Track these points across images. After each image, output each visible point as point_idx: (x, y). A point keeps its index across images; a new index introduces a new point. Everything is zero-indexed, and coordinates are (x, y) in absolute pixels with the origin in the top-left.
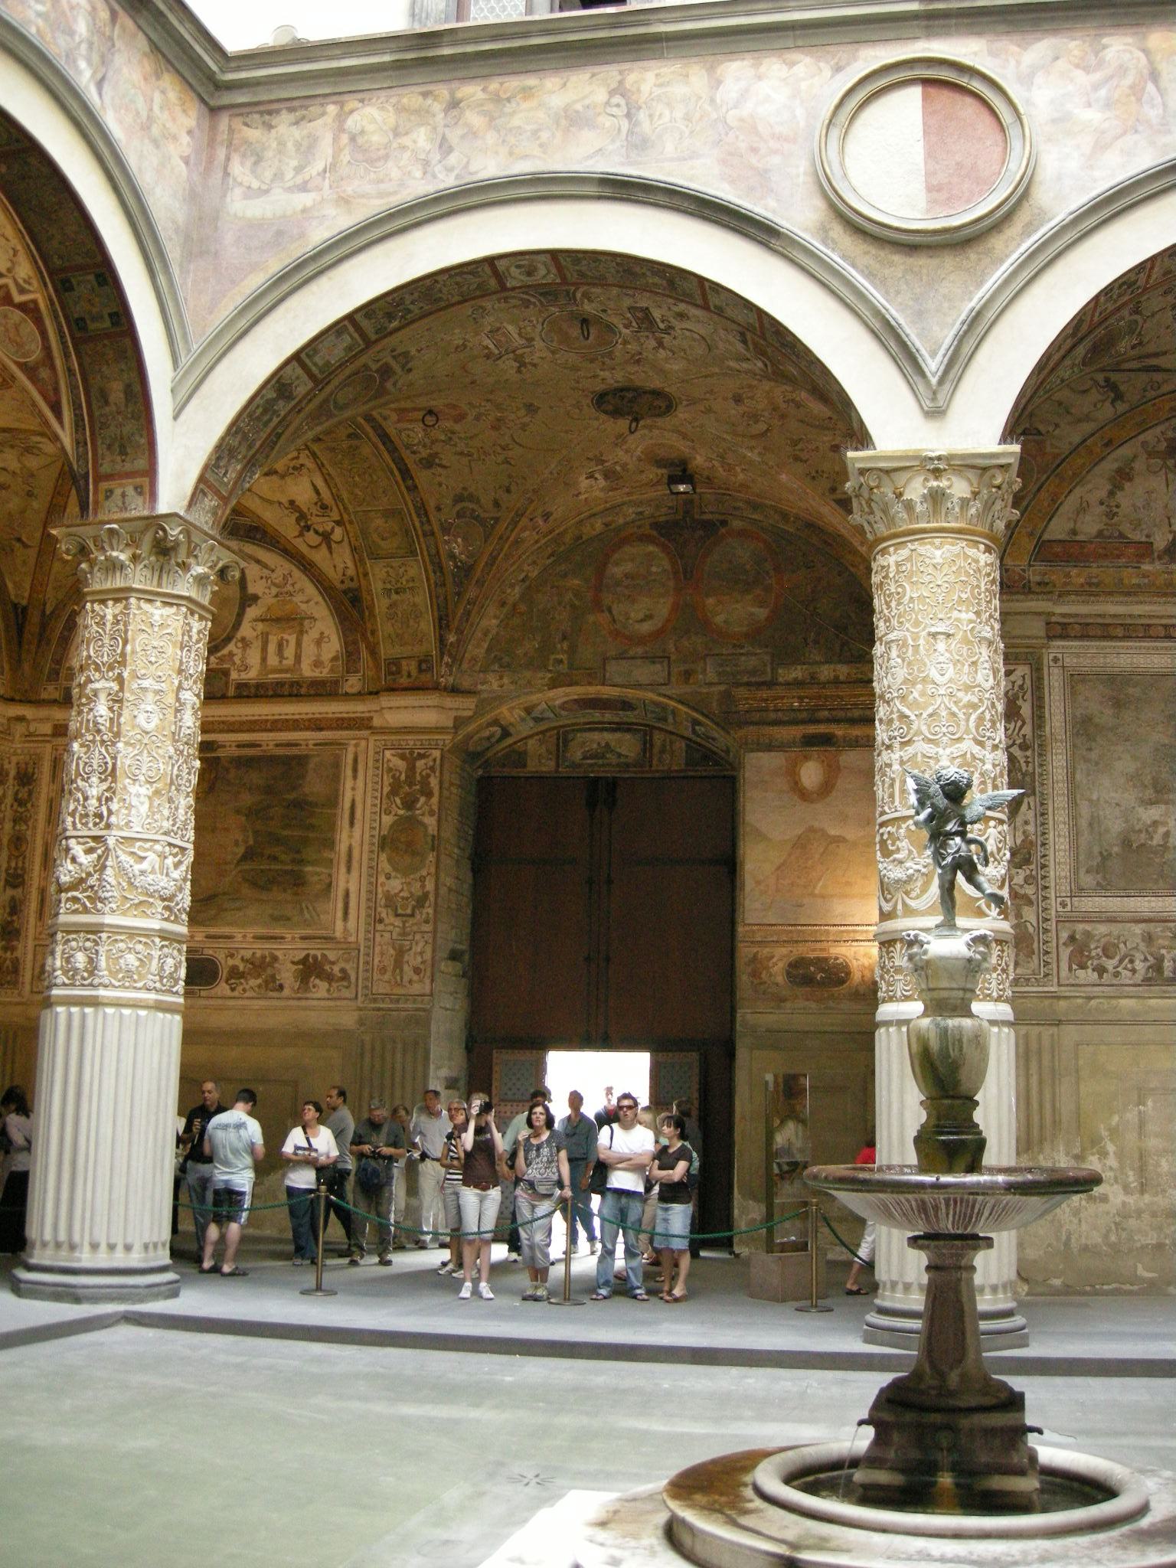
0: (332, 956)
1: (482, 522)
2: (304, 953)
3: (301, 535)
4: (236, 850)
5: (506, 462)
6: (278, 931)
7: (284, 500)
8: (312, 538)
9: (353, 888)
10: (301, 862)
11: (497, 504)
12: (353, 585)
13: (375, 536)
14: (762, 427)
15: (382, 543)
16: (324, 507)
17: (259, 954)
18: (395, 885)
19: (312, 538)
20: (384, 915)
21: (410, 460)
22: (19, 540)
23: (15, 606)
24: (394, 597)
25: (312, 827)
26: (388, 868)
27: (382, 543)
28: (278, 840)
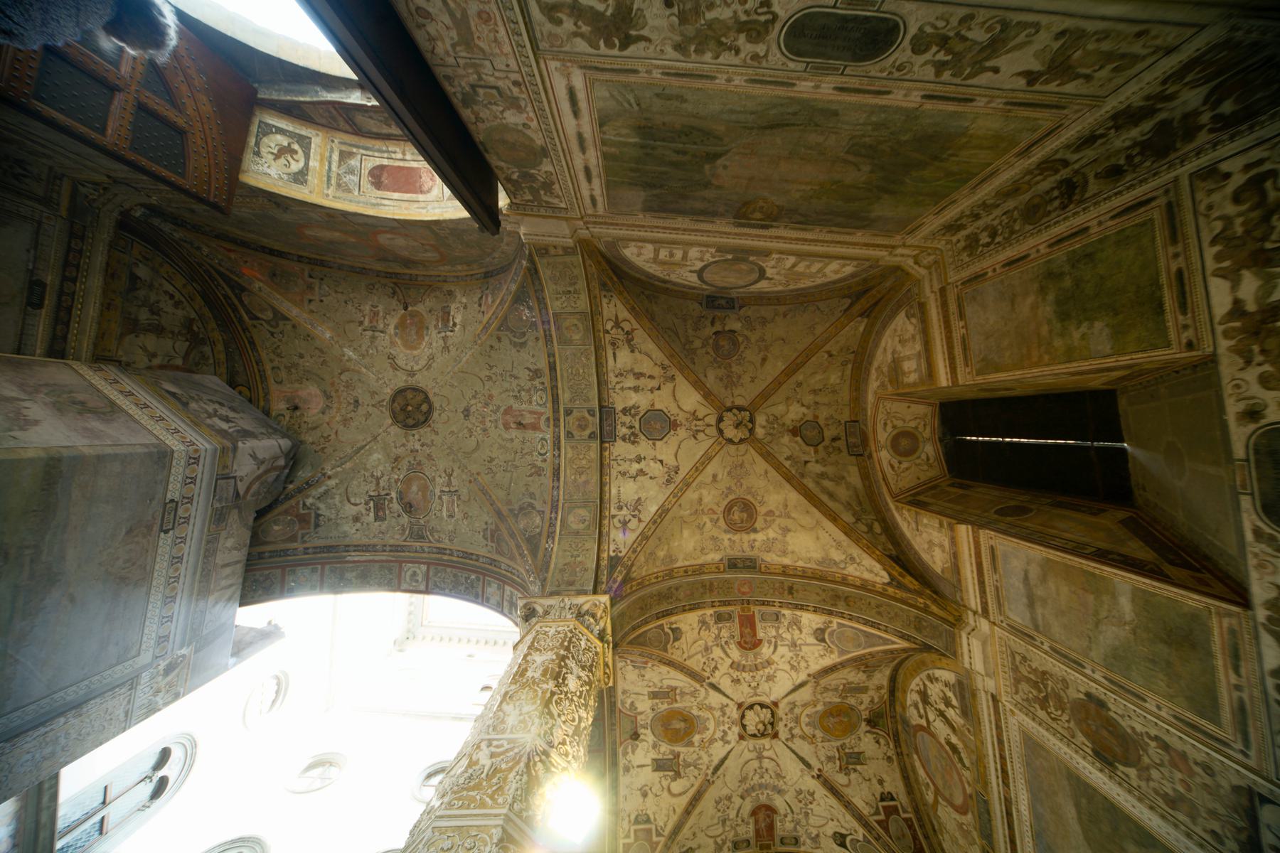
0: (581, 46)
1: (508, 329)
2: (626, 53)
3: (633, 330)
4: (728, 163)
5: (491, 367)
6: (676, 82)
7: (637, 353)
8: (627, 326)
9: (569, 122)
10: (642, 147)
11: (499, 339)
12: (604, 293)
13: (580, 325)
14: (343, 377)
15: (576, 322)
16: (613, 344)
17: (708, 57)
18: (511, 118)
19: (627, 326)
20: (515, 90)
21: (546, 379)
22: (831, 356)
23: (868, 316)
24: (571, 289)
25: (632, 170)
26: (529, 132)
27: (576, 322)
28: (674, 164)
